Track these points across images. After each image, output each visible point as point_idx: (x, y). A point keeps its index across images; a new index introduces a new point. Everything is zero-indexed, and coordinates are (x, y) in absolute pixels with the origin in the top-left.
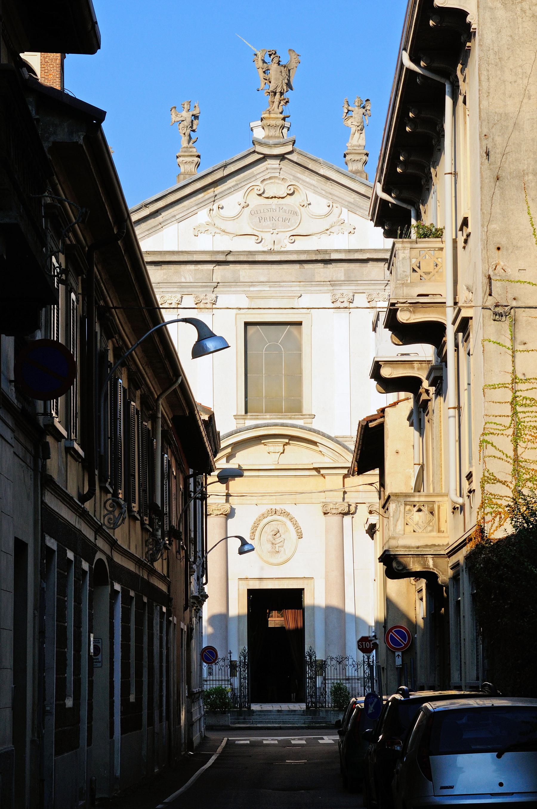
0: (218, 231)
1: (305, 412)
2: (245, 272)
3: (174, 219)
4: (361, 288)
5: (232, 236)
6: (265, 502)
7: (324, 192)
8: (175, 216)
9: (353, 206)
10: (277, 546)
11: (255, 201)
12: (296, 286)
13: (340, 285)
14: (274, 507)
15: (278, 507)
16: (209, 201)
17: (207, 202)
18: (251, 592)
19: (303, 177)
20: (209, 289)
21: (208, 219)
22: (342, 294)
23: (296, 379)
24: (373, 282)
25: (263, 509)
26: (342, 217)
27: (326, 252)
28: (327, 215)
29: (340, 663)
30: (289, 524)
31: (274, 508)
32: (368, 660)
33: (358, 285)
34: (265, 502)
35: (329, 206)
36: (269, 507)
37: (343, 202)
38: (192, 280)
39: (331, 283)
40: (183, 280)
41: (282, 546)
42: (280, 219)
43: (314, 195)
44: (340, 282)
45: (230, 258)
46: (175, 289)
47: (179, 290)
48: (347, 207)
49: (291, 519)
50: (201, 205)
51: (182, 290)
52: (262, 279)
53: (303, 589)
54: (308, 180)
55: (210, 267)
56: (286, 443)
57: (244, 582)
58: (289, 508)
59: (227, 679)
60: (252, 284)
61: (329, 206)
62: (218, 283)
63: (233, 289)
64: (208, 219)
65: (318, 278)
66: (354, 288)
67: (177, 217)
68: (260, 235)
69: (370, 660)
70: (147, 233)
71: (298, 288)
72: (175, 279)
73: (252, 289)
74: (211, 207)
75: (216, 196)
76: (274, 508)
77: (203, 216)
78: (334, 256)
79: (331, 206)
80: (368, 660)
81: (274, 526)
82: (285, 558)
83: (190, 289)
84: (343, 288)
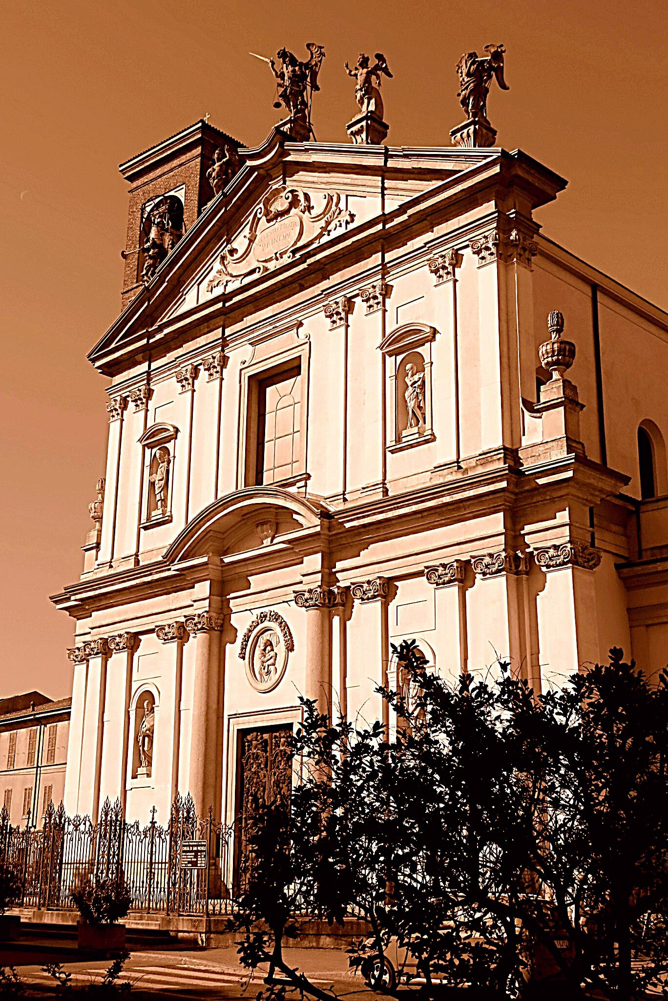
34: (257, 605)
36: (258, 611)
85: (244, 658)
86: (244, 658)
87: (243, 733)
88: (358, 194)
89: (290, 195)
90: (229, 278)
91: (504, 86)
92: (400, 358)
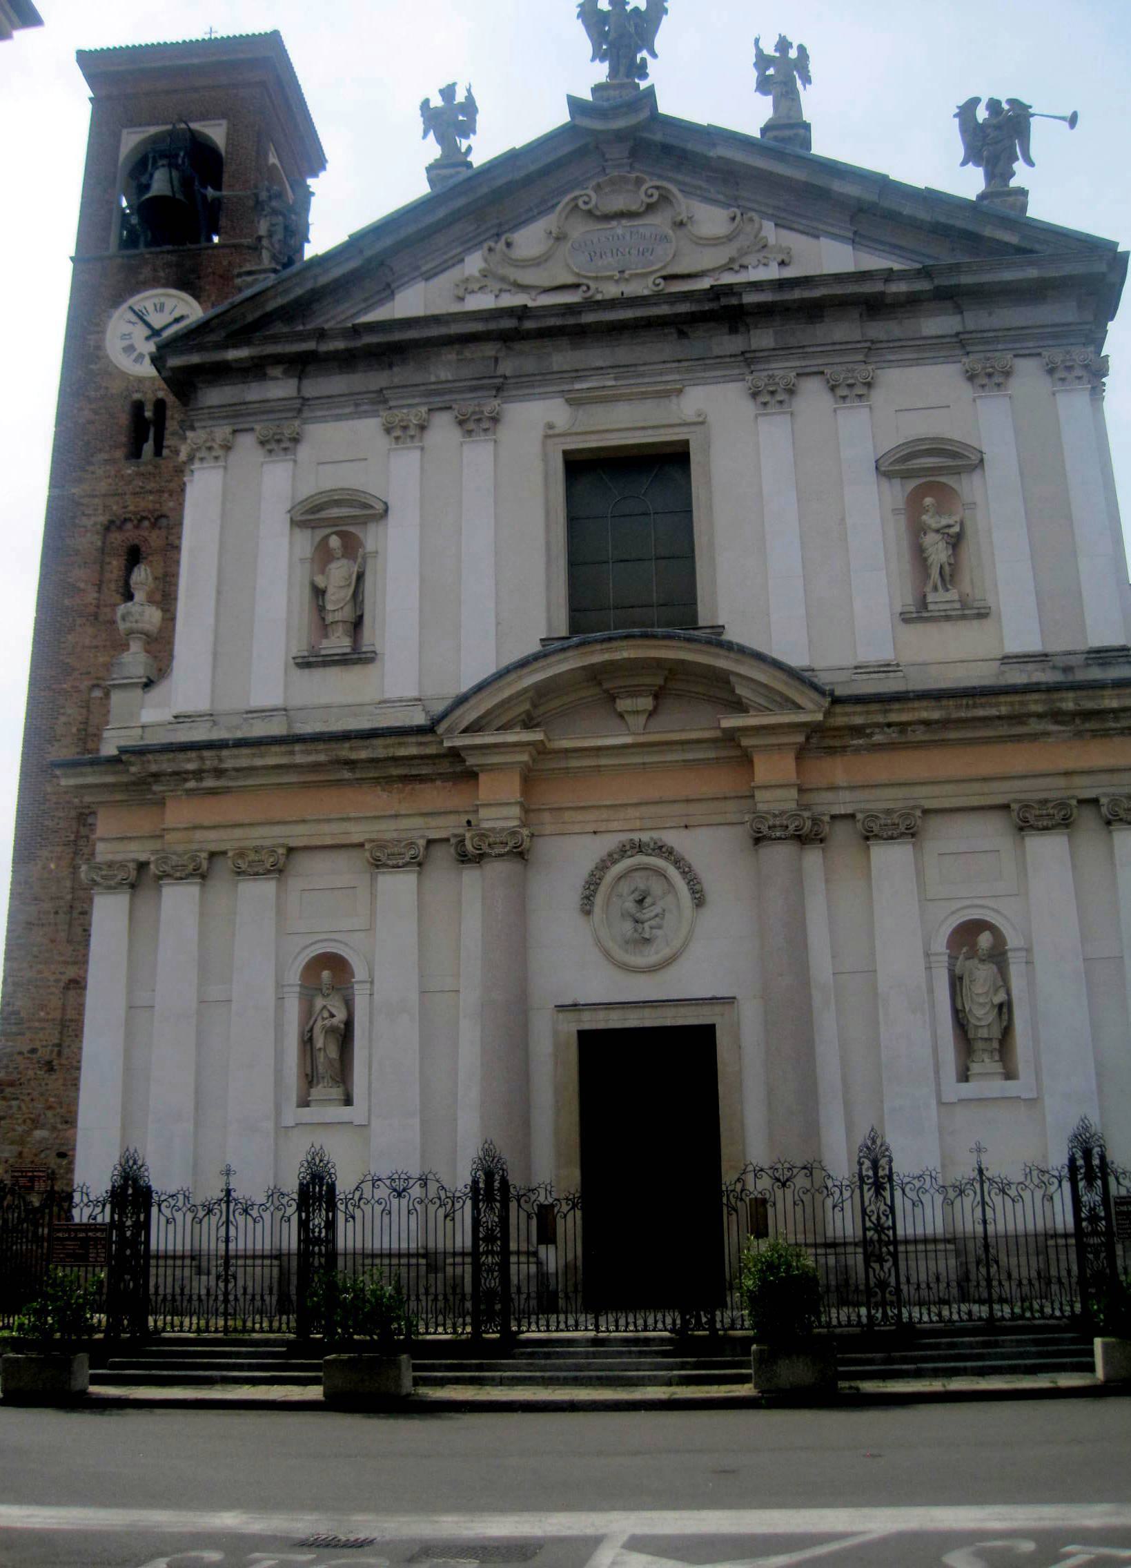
0: (505, 287)
1: (701, 623)
2: (562, 358)
3: (417, 274)
4: (814, 363)
5: (533, 293)
6: (615, 825)
7: (721, 197)
8: (418, 268)
9: (783, 215)
10: (646, 925)
11: (579, 229)
12: (671, 371)
13: (767, 359)
14: (636, 836)
15: (645, 837)
16: (488, 235)
17: (482, 238)
18: (587, 1039)
19: (680, 177)
20: (486, 393)
21: (482, 265)
22: (770, 377)
23: (680, 557)
24: (838, 347)
25: (609, 842)
26: (763, 234)
27: (729, 290)
28: (729, 238)
29: (784, 1185)
30: (672, 872)
31: (637, 839)
32: (876, 1173)
33: (806, 356)
34: (615, 825)
35: (733, 219)
37: (763, 209)
38: (450, 378)
39: (748, 355)
40: (433, 379)
41: (660, 927)
42: (634, 252)
43: (703, 205)
44: (766, 354)
45: (529, 325)
46: (416, 401)
47: (424, 400)
48: (770, 217)
49: (678, 862)
50: (470, 245)
51: (431, 400)
52: (600, 363)
53: (714, 1026)
54: (688, 179)
55: (489, 349)
56: (661, 688)
57: (570, 1016)
58: (671, 838)
59: (524, 1247)
60: (578, 374)
61: (733, 219)
62: (505, 377)
63: (537, 391)
64: (482, 265)
65: (717, 351)
66: (797, 364)
67: (424, 269)
68: (593, 285)
69: (881, 1173)
70: (363, 305)
71: (677, 377)
72: (418, 378)
73: (577, 386)
74: (492, 244)
75: (500, 225)
76: (637, 839)
77: (474, 263)
78: (750, 298)
79: (738, 218)
80: (876, 1173)
81: (639, 881)
82: (666, 952)
83: (447, 397)
84: (774, 366)
85: (588, 913)
86: (588, 913)
87: (587, 1039)
88: (795, 226)
89: (656, 194)
90: (507, 287)
91: (1031, 164)
92: (912, 484)
